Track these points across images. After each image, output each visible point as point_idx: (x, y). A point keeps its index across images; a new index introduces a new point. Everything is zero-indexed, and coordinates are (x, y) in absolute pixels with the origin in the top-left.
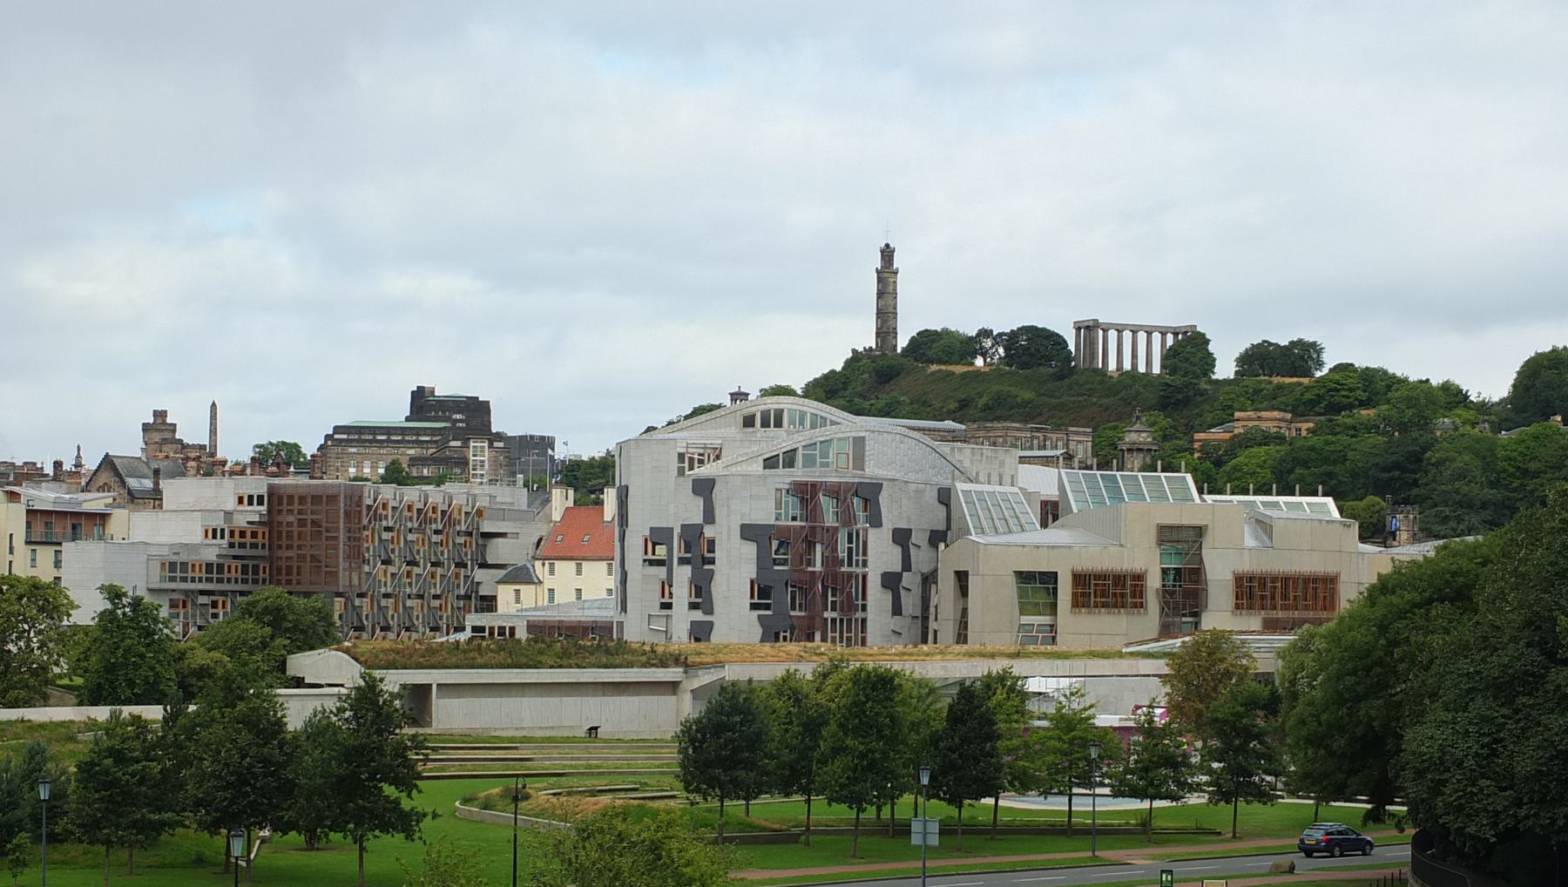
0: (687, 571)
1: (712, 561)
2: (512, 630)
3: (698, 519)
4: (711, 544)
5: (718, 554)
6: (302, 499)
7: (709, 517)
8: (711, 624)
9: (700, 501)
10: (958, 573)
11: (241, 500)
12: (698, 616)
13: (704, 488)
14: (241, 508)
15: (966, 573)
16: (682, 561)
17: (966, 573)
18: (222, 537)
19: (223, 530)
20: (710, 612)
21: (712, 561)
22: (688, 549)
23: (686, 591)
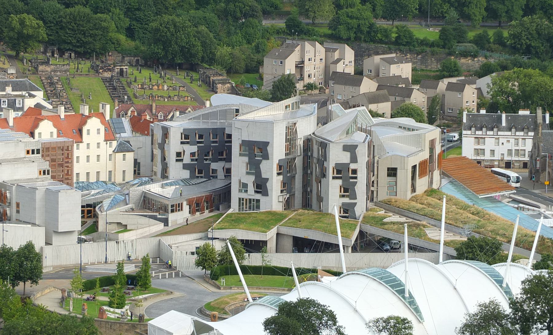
0: (339, 182)
1: (356, 178)
2: (182, 204)
3: (349, 162)
4: (355, 171)
5: (359, 175)
6: (54, 148)
7: (354, 159)
8: (356, 203)
9: (348, 154)
10: (388, 169)
11: (28, 152)
12: (346, 200)
13: (351, 149)
14: (28, 156)
15: (395, 169)
16: (334, 178)
17: (395, 169)
18: (48, 174)
19: (48, 171)
20: (355, 198)
21: (356, 178)
22: (339, 172)
23: (339, 190)
